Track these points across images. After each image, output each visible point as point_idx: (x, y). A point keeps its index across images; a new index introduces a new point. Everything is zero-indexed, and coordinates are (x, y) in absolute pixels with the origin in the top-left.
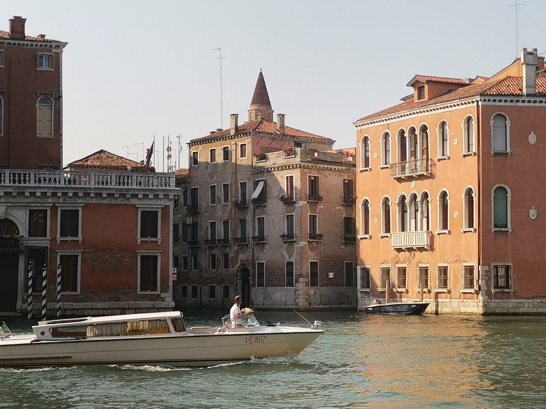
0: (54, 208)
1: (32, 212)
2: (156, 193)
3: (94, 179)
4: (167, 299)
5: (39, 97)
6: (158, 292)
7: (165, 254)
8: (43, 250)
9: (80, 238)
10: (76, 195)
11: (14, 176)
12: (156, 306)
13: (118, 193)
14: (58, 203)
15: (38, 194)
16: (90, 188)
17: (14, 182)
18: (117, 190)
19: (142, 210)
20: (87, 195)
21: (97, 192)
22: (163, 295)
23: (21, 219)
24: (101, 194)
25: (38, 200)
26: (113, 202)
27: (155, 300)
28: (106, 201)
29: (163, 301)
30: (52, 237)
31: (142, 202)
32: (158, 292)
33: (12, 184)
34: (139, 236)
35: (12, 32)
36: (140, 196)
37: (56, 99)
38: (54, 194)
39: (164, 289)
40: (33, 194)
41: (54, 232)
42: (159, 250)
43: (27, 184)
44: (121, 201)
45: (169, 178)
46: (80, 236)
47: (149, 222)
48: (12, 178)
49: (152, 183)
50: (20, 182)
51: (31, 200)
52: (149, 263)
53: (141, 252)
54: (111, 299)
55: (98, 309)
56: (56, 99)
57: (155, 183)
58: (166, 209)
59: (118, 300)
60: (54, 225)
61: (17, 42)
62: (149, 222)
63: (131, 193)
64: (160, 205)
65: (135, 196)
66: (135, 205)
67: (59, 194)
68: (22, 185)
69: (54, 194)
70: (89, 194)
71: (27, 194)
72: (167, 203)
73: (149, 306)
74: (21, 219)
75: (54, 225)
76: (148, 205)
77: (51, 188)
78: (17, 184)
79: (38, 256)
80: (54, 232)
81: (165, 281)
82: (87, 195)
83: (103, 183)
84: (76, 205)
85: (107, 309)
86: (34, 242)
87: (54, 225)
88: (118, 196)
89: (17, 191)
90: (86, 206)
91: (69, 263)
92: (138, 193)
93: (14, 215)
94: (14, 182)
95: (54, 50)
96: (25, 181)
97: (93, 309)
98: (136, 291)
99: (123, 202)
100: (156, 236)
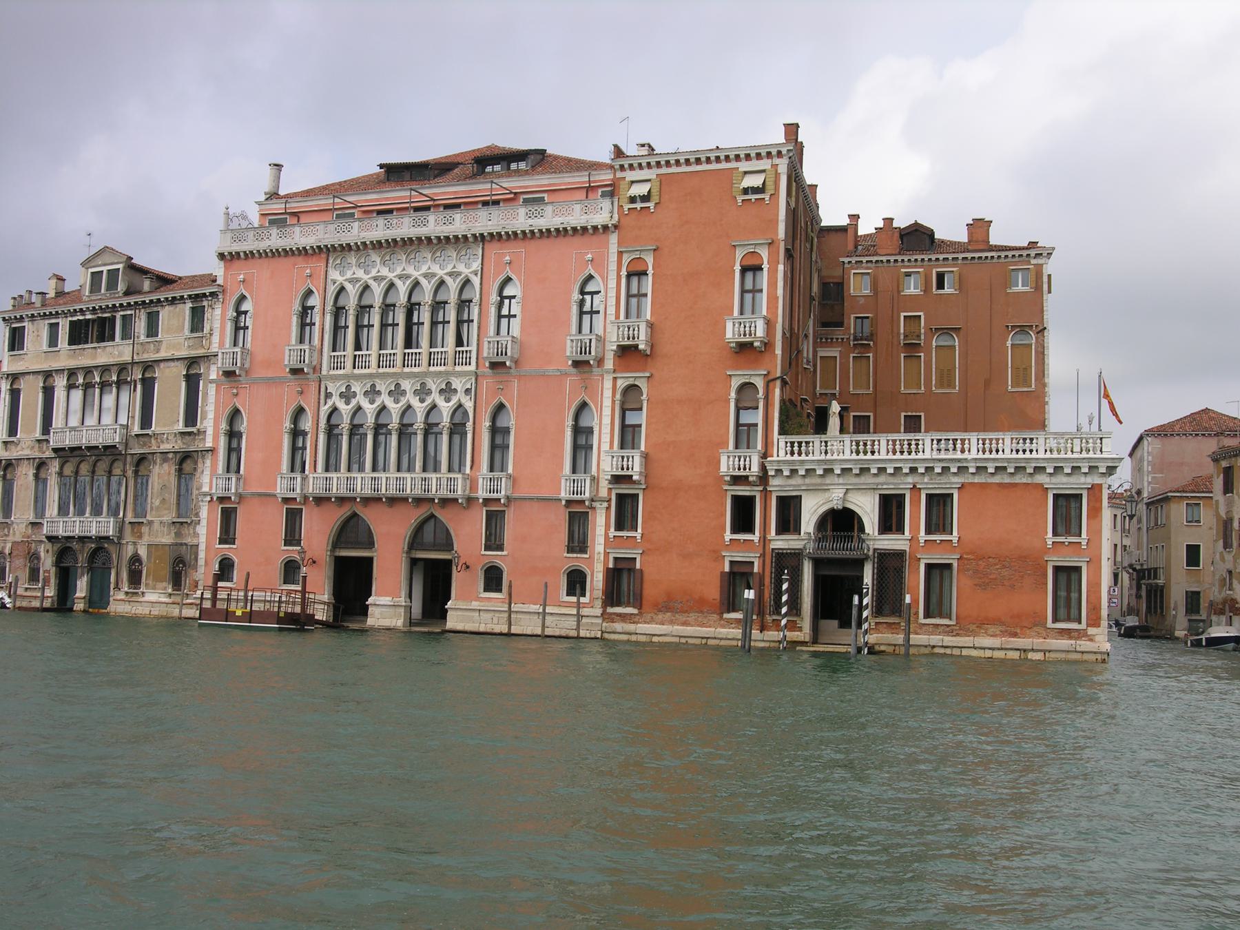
0: (915, 489)
7: (1095, 562)
8: (900, 555)
10: (945, 470)
11: (894, 445)
15: (890, 471)
18: (1009, 460)
20: (962, 470)
22: (1091, 631)
23: (867, 509)
25: (891, 480)
26: (1007, 480)
28: (997, 479)
29: (1091, 640)
30: (913, 534)
31: (1054, 480)
32: (1083, 626)
33: (854, 456)
34: (1050, 534)
35: (970, 241)
36: (1050, 470)
38: (913, 470)
39: (1094, 622)
40: (882, 470)
41: (914, 529)
43: (876, 456)
44: (1020, 479)
46: (955, 533)
47: (1067, 509)
50: (865, 453)
51: (882, 479)
52: (1067, 575)
53: (1055, 560)
57: (1077, 449)
58: (1095, 490)
59: (1015, 635)
60: (915, 515)
61: (977, 255)
62: (1067, 509)
65: (1039, 470)
66: (1042, 485)
67: (921, 470)
68: (869, 456)
69: (913, 470)
71: (874, 471)
72: (1097, 480)
74: (867, 509)
75: (914, 519)
77: (940, 460)
78: (861, 456)
79: (891, 565)
80: (914, 529)
81: (1095, 609)
82: (962, 470)
83: (997, 451)
87: (914, 519)
88: (1051, 471)
95: (1033, 261)
97: (975, 648)
99: (1024, 480)
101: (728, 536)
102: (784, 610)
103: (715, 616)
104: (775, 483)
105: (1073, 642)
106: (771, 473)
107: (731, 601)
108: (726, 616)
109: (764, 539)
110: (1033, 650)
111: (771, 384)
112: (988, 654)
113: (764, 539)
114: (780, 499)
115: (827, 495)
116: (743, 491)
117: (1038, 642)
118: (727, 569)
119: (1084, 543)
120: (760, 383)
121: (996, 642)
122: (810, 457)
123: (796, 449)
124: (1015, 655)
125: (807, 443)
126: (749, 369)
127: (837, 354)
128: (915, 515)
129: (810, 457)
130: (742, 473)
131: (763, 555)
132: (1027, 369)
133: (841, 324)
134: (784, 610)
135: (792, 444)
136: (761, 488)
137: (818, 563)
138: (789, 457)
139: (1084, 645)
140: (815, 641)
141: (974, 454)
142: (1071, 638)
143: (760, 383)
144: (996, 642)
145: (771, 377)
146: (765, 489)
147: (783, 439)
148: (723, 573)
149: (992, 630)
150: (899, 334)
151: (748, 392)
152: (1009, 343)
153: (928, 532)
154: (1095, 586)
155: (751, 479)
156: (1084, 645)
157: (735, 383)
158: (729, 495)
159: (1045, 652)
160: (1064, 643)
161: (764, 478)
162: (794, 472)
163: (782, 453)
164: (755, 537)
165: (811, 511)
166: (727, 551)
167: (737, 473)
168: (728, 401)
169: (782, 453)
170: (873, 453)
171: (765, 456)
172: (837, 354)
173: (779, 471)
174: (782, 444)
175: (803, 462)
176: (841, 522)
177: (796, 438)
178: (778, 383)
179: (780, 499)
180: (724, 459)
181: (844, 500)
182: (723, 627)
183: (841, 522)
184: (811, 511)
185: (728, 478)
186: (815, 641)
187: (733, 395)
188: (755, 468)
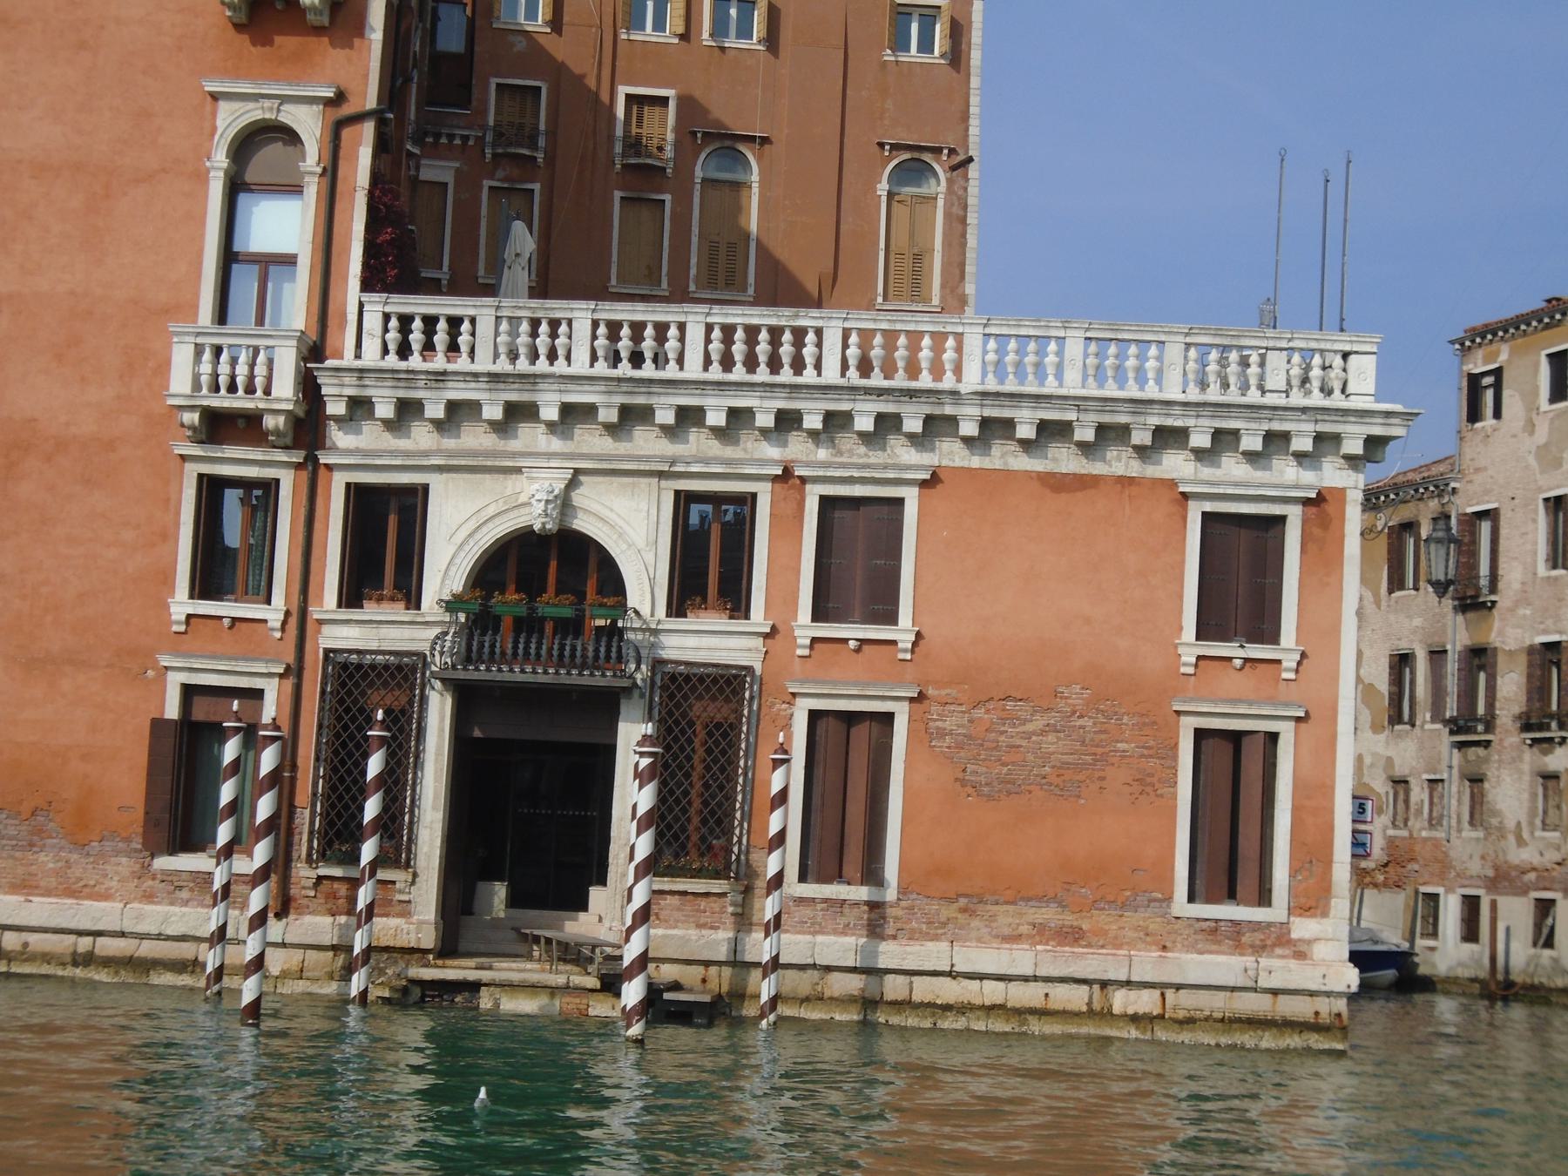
1: (684, 500)
2: (1276, 426)
3: (978, 351)
4: (1319, 951)
5: (890, 159)
6: (1276, 912)
9: (903, 632)
12: (1263, 983)
13: (1093, 418)
14: (808, 465)
16: (954, 393)
17: (615, 359)
18: (1079, 403)
19: (1209, 507)
21: (987, 413)
22: (1303, 928)
23: (634, 532)
24: (1009, 424)
27: (1260, 949)
29: (1300, 955)
32: (1276, 912)
33: (601, 368)
37: (954, 168)
38: (787, 421)
39: (1311, 902)
41: (783, 599)
42: (1287, 705)
45: (1345, 356)
48: (601, 342)
49: (1262, 378)
54: (1041, 933)
55: (981, 977)
56: (954, 168)
57: (1276, 380)
59: (1071, 936)
60: (783, 562)
63: (1155, 421)
64: (1297, 487)
65: (1169, 437)
66: (1173, 483)
68: (648, 371)
70: (953, 421)
73: (1231, 981)
74: (634, 532)
75: (784, 569)
76: (1236, 484)
78: (625, 369)
80: (783, 599)
84: (891, 475)
85: (1026, 979)
86: (692, 641)
87: (784, 569)
89: (620, 399)
90: (932, 482)
91: (848, 748)
92: (1190, 422)
93: (605, 513)
94: (615, 359)
96: (659, 360)
97: (951, 974)
98: (1169, 899)
100: (1273, 637)
101: (182, 604)
102: (368, 851)
103: (126, 865)
104: (339, 437)
105: (1249, 961)
106: (336, 408)
107: (180, 818)
108: (164, 863)
109: (301, 620)
110: (1128, 984)
111: (346, 133)
112: (993, 992)
113: (301, 620)
114: (357, 493)
115: (511, 484)
116: (238, 461)
117: (1147, 965)
118: (172, 711)
119: (1290, 661)
120: (308, 123)
121: (1021, 959)
122: (462, 363)
123: (416, 338)
124: (1076, 998)
125: (455, 323)
126: (277, 79)
127: (448, 177)
128: (783, 562)
129: (462, 363)
130: (239, 402)
131: (295, 672)
132: (919, 259)
133: (465, 102)
134: (368, 851)
135: (406, 321)
136: (297, 457)
137: (467, 698)
138: (392, 360)
139: (1279, 970)
140: (448, 948)
141: (972, 380)
142: (1238, 948)
143: (308, 123)
144: (1021, 959)
145: (347, 110)
146: (312, 459)
147: (376, 305)
148: (158, 724)
149: (1006, 918)
150: (611, 137)
151: (269, 156)
152: (883, 188)
153: (819, 615)
154: (1314, 793)
155: (269, 422)
156: (1279, 970)
157: (230, 120)
158: (192, 471)
159: (1162, 987)
160: (1224, 966)
161: (308, 428)
162: (408, 410)
163: (371, 348)
164: (273, 614)
165: (458, 533)
166: (177, 653)
167: (223, 401)
168: (202, 178)
169: (371, 348)
170: (659, 360)
171: (314, 351)
172: (448, 177)
173: (360, 407)
174: (373, 322)
175: (440, 377)
176: (548, 570)
177: (419, 305)
178: (368, 129)
179: (357, 493)
180: (182, 356)
181: (565, 503)
182: (149, 897)
183: (548, 570)
184: (458, 533)
185: (193, 418)
186: (448, 948)
187: (220, 159)
188: (285, 388)
